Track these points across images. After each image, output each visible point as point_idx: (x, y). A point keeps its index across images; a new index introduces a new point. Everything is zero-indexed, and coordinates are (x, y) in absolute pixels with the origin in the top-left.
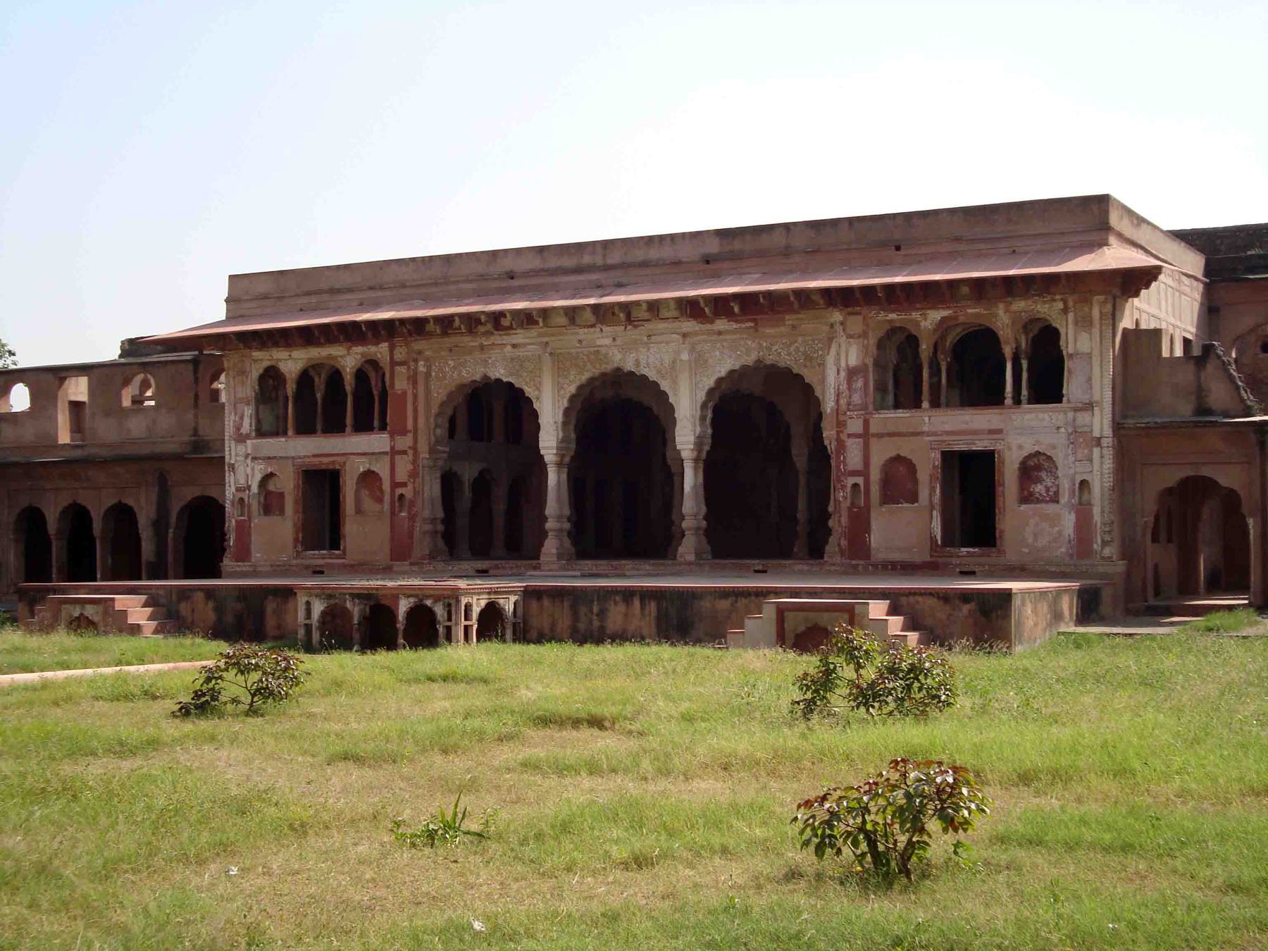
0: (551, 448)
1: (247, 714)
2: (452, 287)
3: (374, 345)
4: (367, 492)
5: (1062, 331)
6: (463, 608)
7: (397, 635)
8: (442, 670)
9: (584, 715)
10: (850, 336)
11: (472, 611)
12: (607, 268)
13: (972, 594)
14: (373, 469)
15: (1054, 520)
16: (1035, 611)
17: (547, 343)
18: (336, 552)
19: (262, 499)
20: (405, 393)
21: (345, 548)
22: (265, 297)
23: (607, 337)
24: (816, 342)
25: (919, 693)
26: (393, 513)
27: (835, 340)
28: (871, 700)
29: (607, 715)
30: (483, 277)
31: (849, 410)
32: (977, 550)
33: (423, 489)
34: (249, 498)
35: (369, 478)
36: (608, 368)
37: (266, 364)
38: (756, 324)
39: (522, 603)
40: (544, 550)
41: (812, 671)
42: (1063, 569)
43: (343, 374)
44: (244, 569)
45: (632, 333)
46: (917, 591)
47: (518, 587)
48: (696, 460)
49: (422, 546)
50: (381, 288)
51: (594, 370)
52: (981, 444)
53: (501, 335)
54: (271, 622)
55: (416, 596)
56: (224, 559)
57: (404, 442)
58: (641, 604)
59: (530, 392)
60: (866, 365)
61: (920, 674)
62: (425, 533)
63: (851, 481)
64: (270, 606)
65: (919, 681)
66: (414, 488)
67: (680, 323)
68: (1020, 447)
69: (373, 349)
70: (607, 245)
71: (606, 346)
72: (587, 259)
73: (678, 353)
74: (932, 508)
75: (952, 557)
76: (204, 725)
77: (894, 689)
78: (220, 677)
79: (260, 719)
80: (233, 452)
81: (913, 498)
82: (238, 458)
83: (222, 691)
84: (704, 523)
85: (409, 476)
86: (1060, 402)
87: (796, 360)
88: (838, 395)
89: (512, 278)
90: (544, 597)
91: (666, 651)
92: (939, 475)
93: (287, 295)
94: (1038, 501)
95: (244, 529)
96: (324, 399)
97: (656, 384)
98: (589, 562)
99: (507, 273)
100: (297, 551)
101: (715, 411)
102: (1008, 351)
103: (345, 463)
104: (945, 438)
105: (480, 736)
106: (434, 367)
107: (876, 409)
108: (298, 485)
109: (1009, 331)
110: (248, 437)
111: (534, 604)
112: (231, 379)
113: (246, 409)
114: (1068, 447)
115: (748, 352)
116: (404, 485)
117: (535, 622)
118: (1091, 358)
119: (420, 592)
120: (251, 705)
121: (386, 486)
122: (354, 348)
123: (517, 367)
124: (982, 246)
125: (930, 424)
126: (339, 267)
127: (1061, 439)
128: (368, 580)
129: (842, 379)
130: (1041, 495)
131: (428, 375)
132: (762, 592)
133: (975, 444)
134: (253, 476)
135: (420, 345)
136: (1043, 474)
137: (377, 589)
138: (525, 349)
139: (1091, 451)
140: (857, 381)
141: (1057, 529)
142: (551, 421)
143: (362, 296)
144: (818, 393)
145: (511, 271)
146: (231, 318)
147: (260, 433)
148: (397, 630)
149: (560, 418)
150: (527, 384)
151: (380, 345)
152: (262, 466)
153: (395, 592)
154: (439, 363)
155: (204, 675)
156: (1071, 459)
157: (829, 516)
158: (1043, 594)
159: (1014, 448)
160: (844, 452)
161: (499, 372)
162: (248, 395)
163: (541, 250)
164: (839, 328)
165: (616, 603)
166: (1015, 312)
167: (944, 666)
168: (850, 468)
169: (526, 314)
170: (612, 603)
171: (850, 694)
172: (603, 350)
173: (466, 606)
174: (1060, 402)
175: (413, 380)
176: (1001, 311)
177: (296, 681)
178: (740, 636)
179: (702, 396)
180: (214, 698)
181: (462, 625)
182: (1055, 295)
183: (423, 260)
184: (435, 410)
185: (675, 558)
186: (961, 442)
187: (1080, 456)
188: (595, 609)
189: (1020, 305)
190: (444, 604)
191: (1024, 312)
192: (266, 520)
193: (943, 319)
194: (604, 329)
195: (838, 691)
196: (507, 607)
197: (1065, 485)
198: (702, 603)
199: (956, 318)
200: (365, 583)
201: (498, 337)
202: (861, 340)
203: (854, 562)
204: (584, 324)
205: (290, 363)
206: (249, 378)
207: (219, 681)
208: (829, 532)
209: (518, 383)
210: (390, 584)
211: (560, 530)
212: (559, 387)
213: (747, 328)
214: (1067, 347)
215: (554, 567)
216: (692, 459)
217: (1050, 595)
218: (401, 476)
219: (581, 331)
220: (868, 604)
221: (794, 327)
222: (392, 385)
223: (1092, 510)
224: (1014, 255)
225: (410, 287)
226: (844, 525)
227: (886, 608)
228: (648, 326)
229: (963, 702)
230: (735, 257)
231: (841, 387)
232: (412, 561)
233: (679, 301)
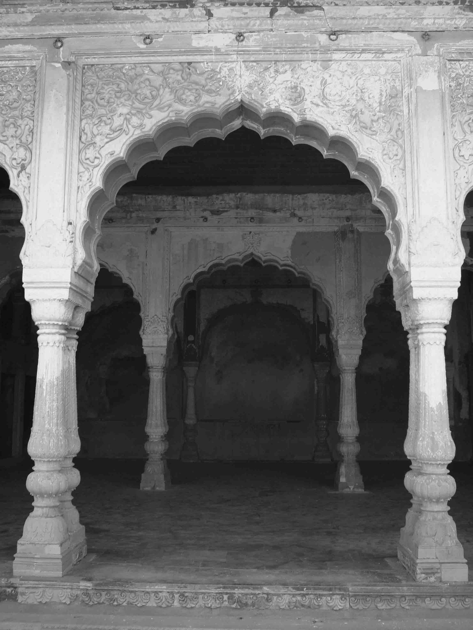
17: (59, 39)
194: (214, 11)
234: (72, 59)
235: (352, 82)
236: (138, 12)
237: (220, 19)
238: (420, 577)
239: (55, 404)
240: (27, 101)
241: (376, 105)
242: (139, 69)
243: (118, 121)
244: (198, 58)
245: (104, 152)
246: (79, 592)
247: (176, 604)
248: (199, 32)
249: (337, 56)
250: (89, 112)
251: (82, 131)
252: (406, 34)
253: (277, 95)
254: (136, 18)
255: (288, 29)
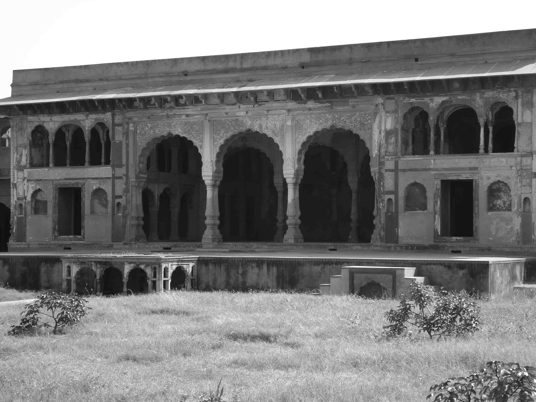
0: (209, 176)
1: (55, 332)
2: (150, 80)
3: (103, 114)
4: (98, 202)
5: (515, 110)
6: (163, 270)
7: (123, 286)
8: (159, 307)
9: (257, 334)
10: (387, 112)
11: (168, 272)
12: (243, 70)
13: (465, 264)
14: (101, 187)
15: (509, 221)
16: (501, 275)
18: (79, 237)
19: (33, 205)
20: (121, 143)
21: (84, 233)
22: (36, 84)
23: (242, 111)
24: (367, 115)
25: (460, 322)
26: (113, 214)
27: (378, 115)
28: (432, 326)
29: (272, 333)
30: (168, 75)
31: (386, 156)
32: (462, 238)
33: (132, 199)
34: (25, 204)
35: (99, 193)
36: (243, 129)
37: (36, 124)
38: (332, 105)
39: (196, 266)
40: (204, 236)
41: (396, 309)
42: (514, 250)
43: (84, 131)
44: (22, 246)
45: (257, 108)
46: (432, 262)
47: (194, 258)
48: (295, 184)
49: (131, 233)
50: (107, 80)
51: (235, 131)
52: (465, 176)
53: (179, 109)
54: (43, 278)
55: (135, 263)
56: (10, 240)
57: (121, 172)
58: (268, 267)
59: (196, 143)
60: (397, 129)
61: (460, 311)
62: (132, 226)
63: (387, 197)
64: (43, 269)
65: (460, 315)
66: (126, 198)
67: (286, 103)
68: (489, 178)
69: (101, 116)
70: (243, 56)
71: (242, 116)
72: (231, 65)
73: (286, 121)
74: (435, 213)
75: (446, 242)
76: (27, 340)
77: (445, 320)
78: (37, 311)
79: (63, 336)
80: (16, 176)
81: (424, 207)
82: (19, 180)
83: (39, 319)
84: (299, 221)
85: (123, 192)
86: (513, 151)
87: (355, 126)
88: (380, 147)
89: (186, 75)
90: (210, 264)
91: (281, 296)
92: (440, 194)
93: (49, 83)
94: (499, 210)
95: (22, 223)
96: (71, 145)
97: (271, 139)
98: (231, 243)
99: (183, 72)
100: (55, 236)
101: (306, 155)
102: (481, 121)
103: (84, 184)
104: (443, 172)
105: (203, 346)
106: (138, 127)
107: (402, 155)
108: (56, 196)
109: (482, 109)
110: (25, 167)
111: (204, 268)
112: (14, 133)
113: (24, 151)
114: (517, 179)
115: (327, 120)
116: (120, 197)
117: (204, 279)
118: (532, 125)
119: (137, 261)
120: (55, 327)
121: (110, 198)
122: (90, 115)
123: (189, 128)
124: (467, 59)
125: (435, 164)
126: (81, 67)
127: (513, 173)
128: (113, 253)
129: (382, 137)
130: (500, 206)
131: (135, 132)
132: (340, 262)
133: (461, 176)
134: (27, 191)
135: (130, 114)
136: (502, 194)
137: (111, 259)
138: (194, 117)
139: (531, 181)
140: (392, 137)
141: (510, 226)
142: (209, 160)
143: (95, 84)
144: (368, 145)
145: (186, 71)
146: (14, 96)
147: (32, 165)
148: (122, 283)
149: (214, 159)
150: (194, 138)
151: (107, 114)
152: (33, 185)
153: (122, 261)
154: (142, 125)
155: (28, 309)
156: (519, 185)
157: (374, 217)
158: (506, 264)
159: (485, 179)
160: (383, 180)
161: (178, 131)
162: (25, 143)
163: (204, 59)
164: (381, 107)
165: (252, 267)
166: (486, 98)
167: (474, 306)
168: (386, 189)
169: (195, 96)
170: (250, 268)
171: (416, 323)
172: (240, 119)
173: (164, 269)
174: (513, 151)
175: (126, 134)
176: (478, 98)
177: (83, 313)
178: (328, 287)
179: (298, 147)
180: (34, 323)
181: (163, 280)
182: (511, 88)
183: (132, 63)
184: (139, 153)
185: (282, 242)
186: (452, 175)
187: (524, 182)
188: (240, 271)
189: (489, 94)
190: (151, 268)
191: (492, 98)
192: (36, 217)
193: (443, 102)
194: (241, 106)
195: (409, 320)
196: (188, 270)
197: (515, 200)
198: (304, 268)
199: (451, 101)
200: (103, 255)
201: (178, 110)
202: (394, 114)
203: (388, 245)
204: (231, 103)
205: (51, 123)
206: (26, 132)
207: (37, 313)
208: (373, 227)
209: (189, 137)
210: (118, 256)
211: (214, 225)
212: (214, 140)
213: (326, 106)
214: (517, 119)
215: (212, 246)
216: (294, 184)
217: (510, 265)
218: (119, 191)
219: (228, 108)
220: (404, 269)
221: (354, 107)
222: (114, 138)
223: (531, 215)
224: (486, 65)
225: (125, 79)
226: (383, 223)
227: (414, 272)
228: (267, 105)
229: (484, 329)
230: (319, 64)
231: (382, 142)
232: (124, 242)
233: (286, 90)
234: (210, 119)
235: (273, 123)
236: (223, 107)
237: (242, 108)
238: (284, 242)
239: (210, 204)
240: (201, 130)
241: (278, 129)
242: (225, 121)
243: (222, 135)
244: (239, 118)
245: (219, 143)
246: (214, 245)
247: (234, 247)
248: (238, 112)
249: (270, 116)
250: (215, 132)
251: (214, 137)
252: (284, 110)
253: (256, 127)
254: (224, 109)
255: (257, 110)
